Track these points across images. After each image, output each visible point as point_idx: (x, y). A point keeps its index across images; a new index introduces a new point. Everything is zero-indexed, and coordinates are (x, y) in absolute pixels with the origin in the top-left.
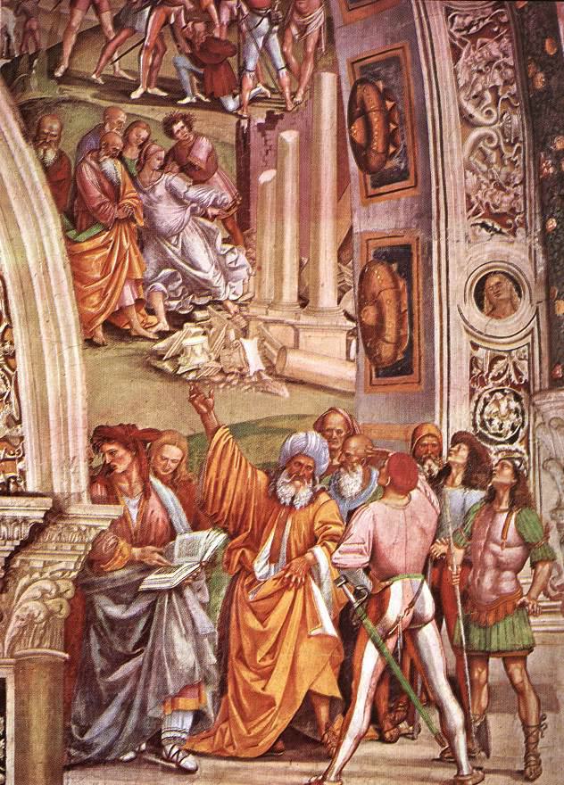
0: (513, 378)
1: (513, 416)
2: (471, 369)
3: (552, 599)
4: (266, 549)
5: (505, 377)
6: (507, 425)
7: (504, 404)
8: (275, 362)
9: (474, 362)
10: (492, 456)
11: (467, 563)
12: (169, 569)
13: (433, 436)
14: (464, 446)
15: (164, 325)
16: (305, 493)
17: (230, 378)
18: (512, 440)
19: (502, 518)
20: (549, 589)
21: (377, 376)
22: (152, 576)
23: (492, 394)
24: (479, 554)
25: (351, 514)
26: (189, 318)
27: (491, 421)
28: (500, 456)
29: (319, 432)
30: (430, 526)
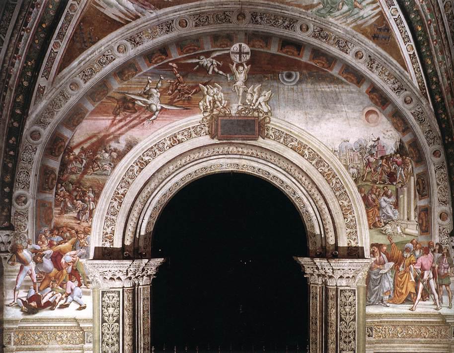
11: (438, 268)
15: (383, 225)
25: (417, 259)
26: (388, 223)
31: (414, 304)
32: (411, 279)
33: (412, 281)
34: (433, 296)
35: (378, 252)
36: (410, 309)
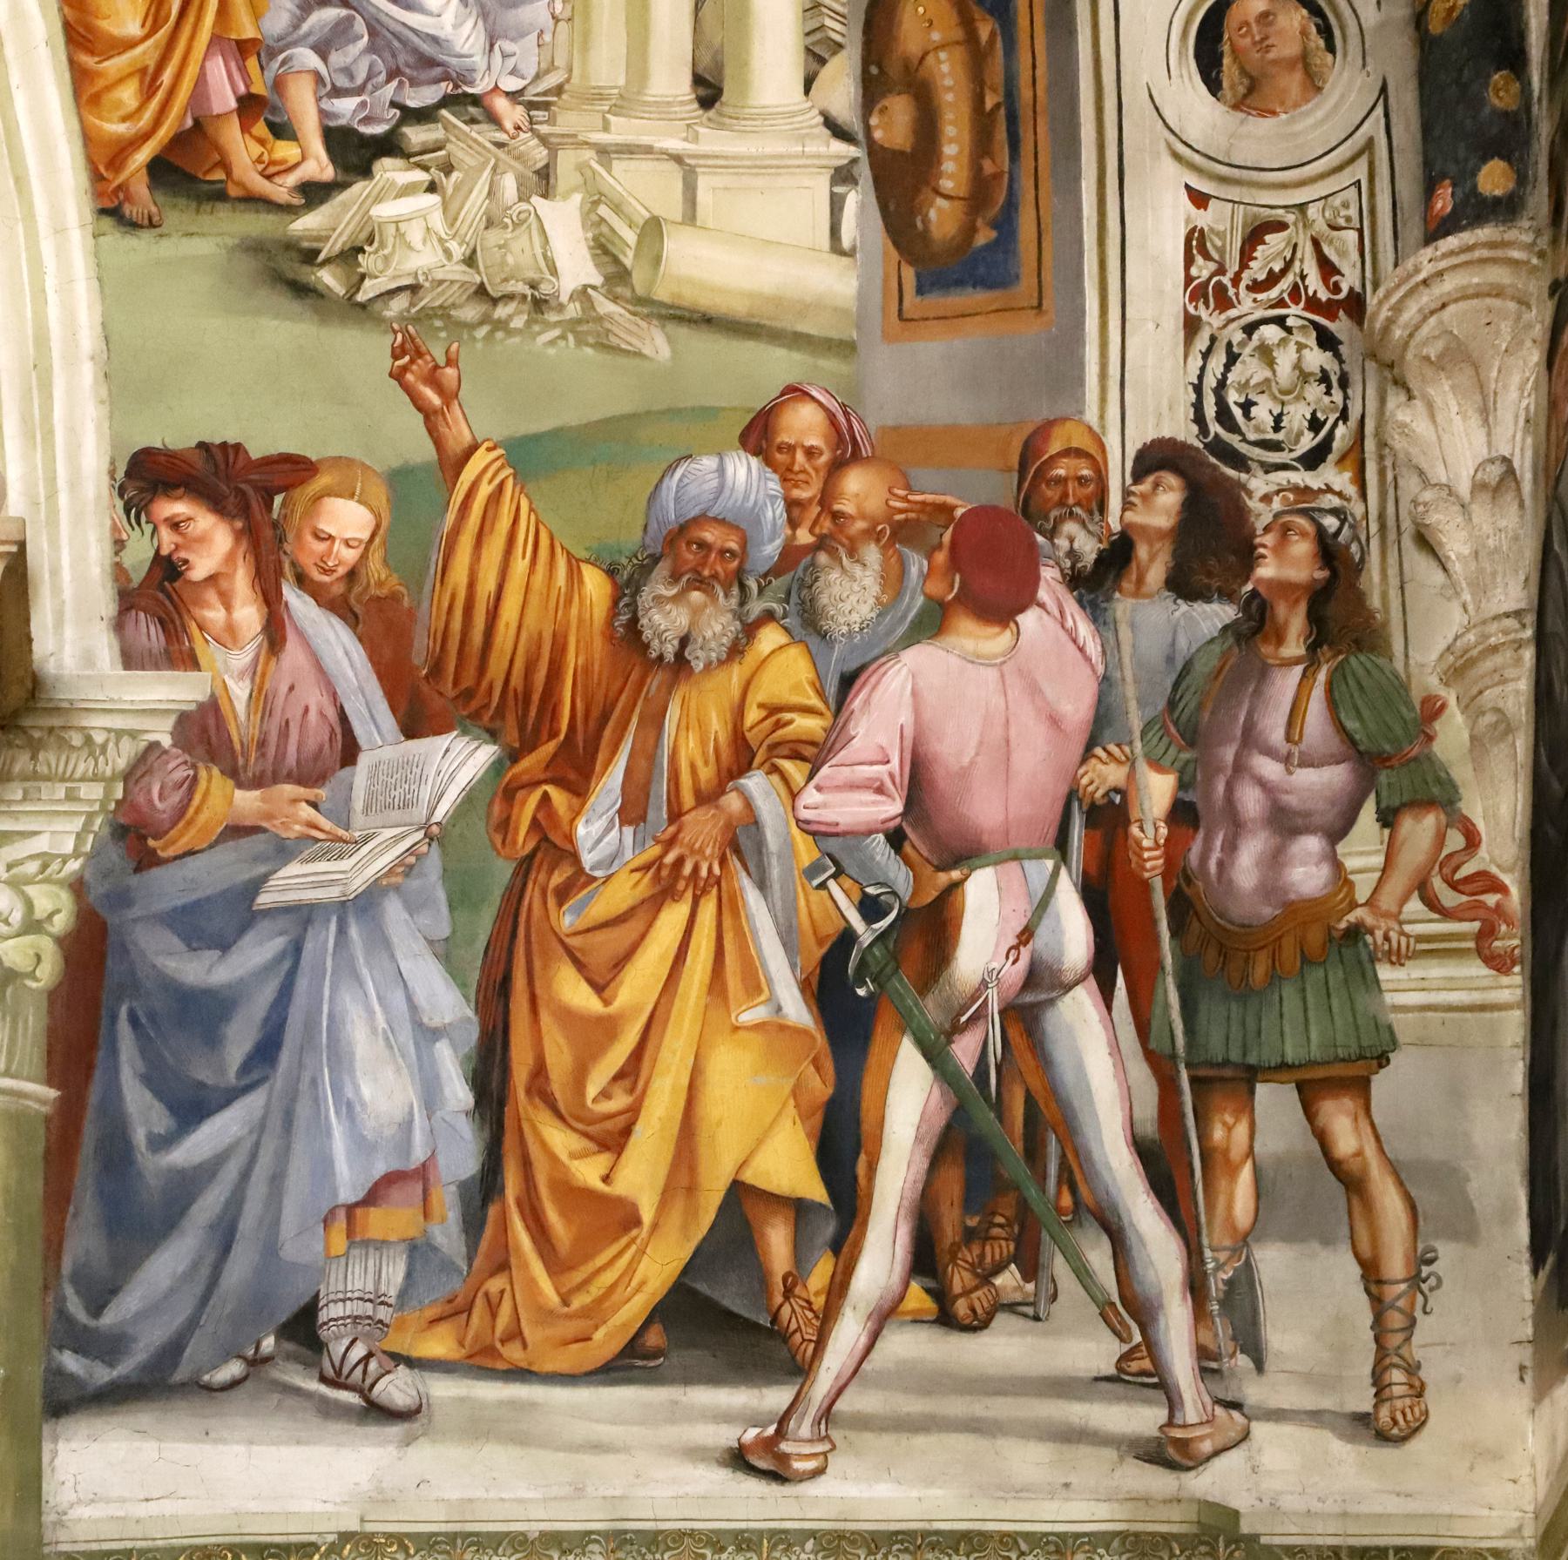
0: (1314, 283)
1: (1314, 391)
2: (1189, 261)
3: (1446, 914)
4: (610, 784)
5: (1285, 284)
6: (1297, 415)
7: (1285, 360)
8: (628, 261)
9: (1196, 243)
10: (1254, 504)
11: (1183, 814)
12: (342, 845)
13: (1079, 453)
14: (1171, 479)
15: (319, 166)
16: (718, 626)
17: (501, 312)
18: (1313, 459)
19: (1286, 683)
20: (1437, 884)
21: (920, 291)
22: (294, 868)
23: (1250, 329)
24: (1220, 788)
25: (848, 682)
26: (389, 146)
27: (1247, 406)
28: (1277, 505)
29: (756, 452)
30: (1077, 707)
31: (800, 1370)
32: (754, 983)
33: (776, 1028)
34: (1099, 1258)
35: (242, 581)
36: (738, 1459)
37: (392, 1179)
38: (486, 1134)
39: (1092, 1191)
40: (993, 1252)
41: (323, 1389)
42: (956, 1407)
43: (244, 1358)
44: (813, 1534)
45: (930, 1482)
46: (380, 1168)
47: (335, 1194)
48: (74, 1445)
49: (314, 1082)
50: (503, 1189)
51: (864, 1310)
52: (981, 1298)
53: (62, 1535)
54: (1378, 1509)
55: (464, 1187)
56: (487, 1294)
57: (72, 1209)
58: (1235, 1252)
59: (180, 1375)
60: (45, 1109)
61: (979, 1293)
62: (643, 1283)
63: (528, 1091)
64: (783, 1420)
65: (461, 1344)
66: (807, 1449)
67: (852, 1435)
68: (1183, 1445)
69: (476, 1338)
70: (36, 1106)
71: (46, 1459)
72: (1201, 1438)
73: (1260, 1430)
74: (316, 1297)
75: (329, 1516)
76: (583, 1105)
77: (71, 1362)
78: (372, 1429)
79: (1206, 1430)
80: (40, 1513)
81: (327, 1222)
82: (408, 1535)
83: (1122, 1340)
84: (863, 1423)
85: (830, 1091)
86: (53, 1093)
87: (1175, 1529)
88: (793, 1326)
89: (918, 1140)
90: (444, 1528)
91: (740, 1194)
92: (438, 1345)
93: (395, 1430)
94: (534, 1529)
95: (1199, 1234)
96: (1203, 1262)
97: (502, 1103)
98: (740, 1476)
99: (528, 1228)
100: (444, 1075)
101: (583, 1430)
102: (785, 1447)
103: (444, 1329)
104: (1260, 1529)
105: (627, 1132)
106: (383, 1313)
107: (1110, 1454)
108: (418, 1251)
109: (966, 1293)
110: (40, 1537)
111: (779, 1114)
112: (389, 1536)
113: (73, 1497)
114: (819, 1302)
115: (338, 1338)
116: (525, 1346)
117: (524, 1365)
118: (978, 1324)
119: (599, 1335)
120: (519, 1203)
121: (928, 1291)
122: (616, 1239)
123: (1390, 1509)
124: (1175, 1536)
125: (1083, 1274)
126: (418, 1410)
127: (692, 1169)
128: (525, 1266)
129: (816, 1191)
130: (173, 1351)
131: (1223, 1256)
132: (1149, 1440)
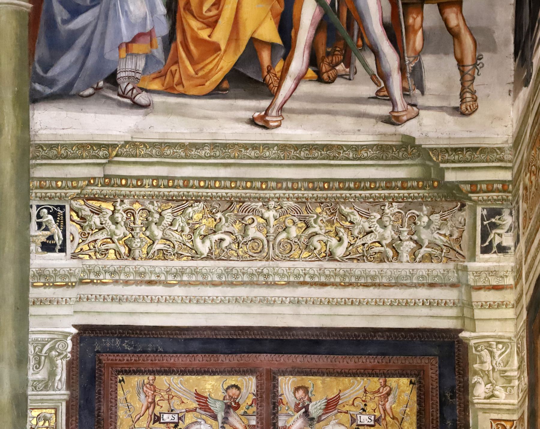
31: (273, 95)
34: (371, 61)
36: (253, 122)
37: (140, 35)
38: (171, 22)
39: (369, 40)
40: (335, 59)
41: (119, 98)
42: (323, 106)
43: (93, 88)
44: (277, 145)
45: (314, 130)
46: (136, 32)
47: (122, 39)
48: (40, 112)
49: (115, 5)
50: (176, 39)
51: (293, 77)
52: (332, 73)
53: (36, 138)
54: (461, 136)
55: (163, 38)
56: (171, 71)
57: (37, 41)
58: (415, 58)
59: (73, 92)
60: (29, 10)
61: (331, 72)
62: (222, 68)
63: (184, 9)
64: (267, 110)
65: (163, 85)
66: (275, 119)
67: (289, 115)
68: (397, 118)
69: (168, 84)
70: (26, 9)
71: (31, 115)
72: (403, 116)
73: (422, 112)
74: (116, 70)
75: (121, 136)
76: (202, 13)
77: (38, 87)
78: (135, 111)
79: (404, 113)
80: (29, 132)
81: (120, 47)
82: (146, 143)
83: (378, 86)
84: (292, 111)
85: (283, 9)
86: (31, 6)
87: (394, 143)
88: (270, 82)
89: (311, 24)
90: (158, 141)
91: (253, 41)
92: (156, 86)
93: (142, 111)
94: (187, 142)
95: (404, 52)
96: (405, 61)
97: (176, 12)
98: (253, 127)
99: (184, 51)
100: (157, 3)
101: (202, 112)
102: (268, 118)
103: (157, 81)
104: (422, 143)
105: (216, 22)
106: (138, 76)
107: (373, 121)
108: (149, 57)
109: (327, 72)
110: (30, 139)
111: (266, 16)
112: (140, 142)
113: (40, 127)
114: (279, 75)
115: (123, 83)
116: (183, 86)
117: (183, 92)
118: (330, 81)
119: (207, 84)
120: (181, 43)
121: (314, 71)
122: (214, 54)
123: (465, 136)
124: (395, 146)
125: (365, 66)
126: (149, 105)
127: (238, 33)
128: (183, 62)
129: (278, 40)
130: (70, 85)
131: (411, 59)
132: (386, 116)
